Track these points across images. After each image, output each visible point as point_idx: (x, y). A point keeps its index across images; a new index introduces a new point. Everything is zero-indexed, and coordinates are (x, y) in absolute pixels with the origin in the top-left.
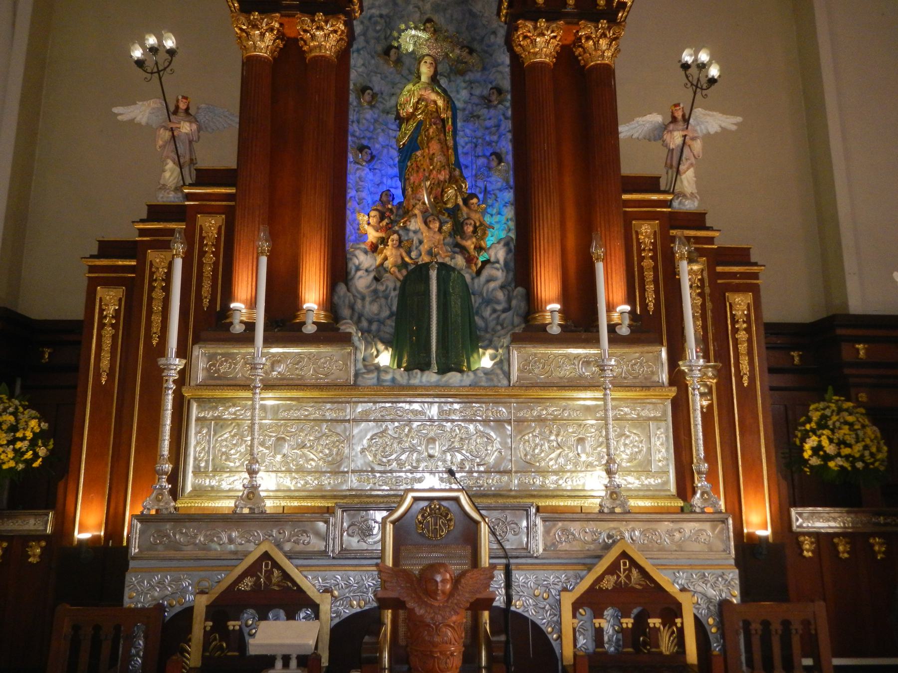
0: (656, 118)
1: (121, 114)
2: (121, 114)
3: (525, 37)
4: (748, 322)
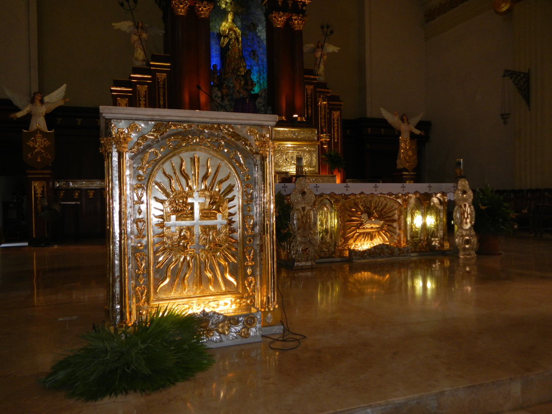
0: (312, 45)
1: (115, 26)
2: (115, 26)
3: (275, 17)
4: (338, 120)
